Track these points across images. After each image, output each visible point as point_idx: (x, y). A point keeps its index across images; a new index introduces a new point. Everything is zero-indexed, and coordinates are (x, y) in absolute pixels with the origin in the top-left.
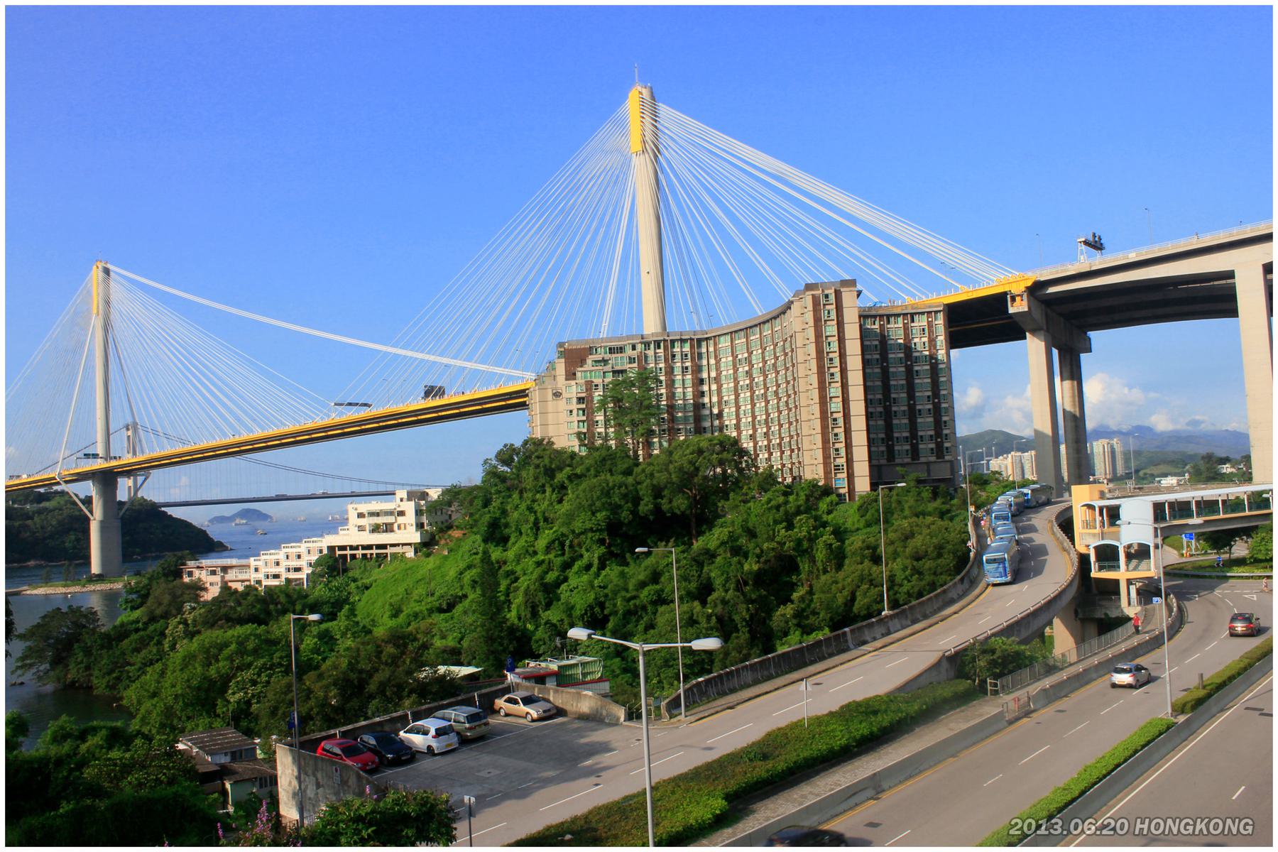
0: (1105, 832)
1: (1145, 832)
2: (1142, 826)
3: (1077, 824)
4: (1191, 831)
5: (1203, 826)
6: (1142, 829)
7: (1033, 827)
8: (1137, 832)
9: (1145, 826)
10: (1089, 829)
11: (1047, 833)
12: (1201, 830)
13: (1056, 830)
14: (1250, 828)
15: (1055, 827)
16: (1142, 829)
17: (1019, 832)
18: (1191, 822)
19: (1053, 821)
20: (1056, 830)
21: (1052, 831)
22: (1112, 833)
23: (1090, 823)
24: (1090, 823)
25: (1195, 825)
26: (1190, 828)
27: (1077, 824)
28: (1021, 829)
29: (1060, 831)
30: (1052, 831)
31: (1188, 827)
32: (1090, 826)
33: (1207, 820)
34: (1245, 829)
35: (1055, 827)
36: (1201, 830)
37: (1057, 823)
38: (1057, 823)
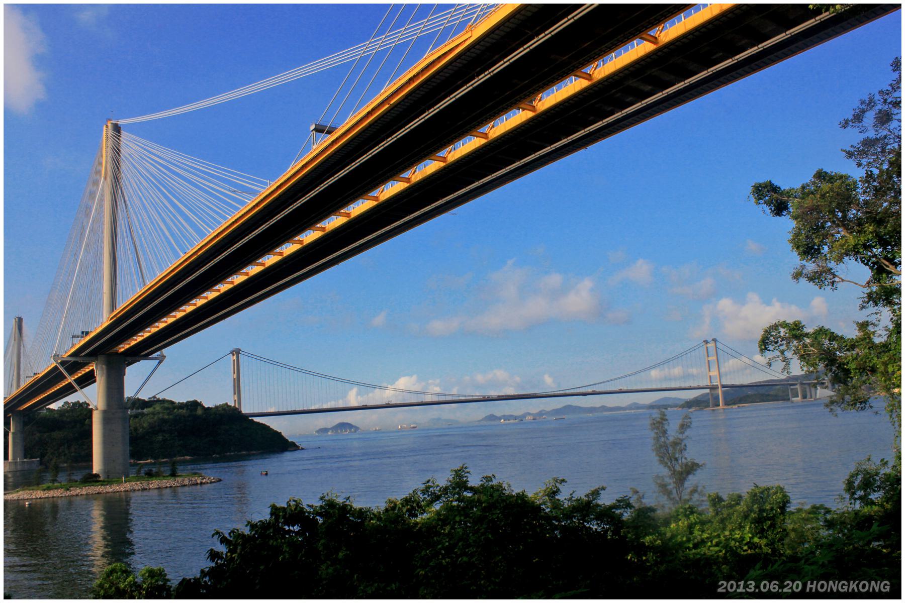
0: (785, 590)
1: (814, 590)
2: (811, 586)
3: (765, 586)
4: (846, 590)
5: (855, 586)
6: (811, 589)
7: (735, 587)
8: (808, 590)
9: (814, 586)
10: (774, 588)
11: (744, 591)
12: (853, 589)
13: (751, 589)
14: (888, 588)
15: (750, 586)
16: (811, 589)
17: (724, 591)
18: (846, 583)
19: (749, 583)
20: (751, 589)
21: (748, 590)
22: (790, 591)
23: (775, 584)
24: (775, 584)
25: (849, 585)
26: (846, 587)
27: (765, 585)
28: (726, 588)
29: (752, 590)
30: (748, 590)
31: (844, 587)
32: (775, 586)
33: (857, 582)
34: (884, 588)
35: (750, 586)
36: (853, 589)
37: (751, 584)
38: (751, 584)
